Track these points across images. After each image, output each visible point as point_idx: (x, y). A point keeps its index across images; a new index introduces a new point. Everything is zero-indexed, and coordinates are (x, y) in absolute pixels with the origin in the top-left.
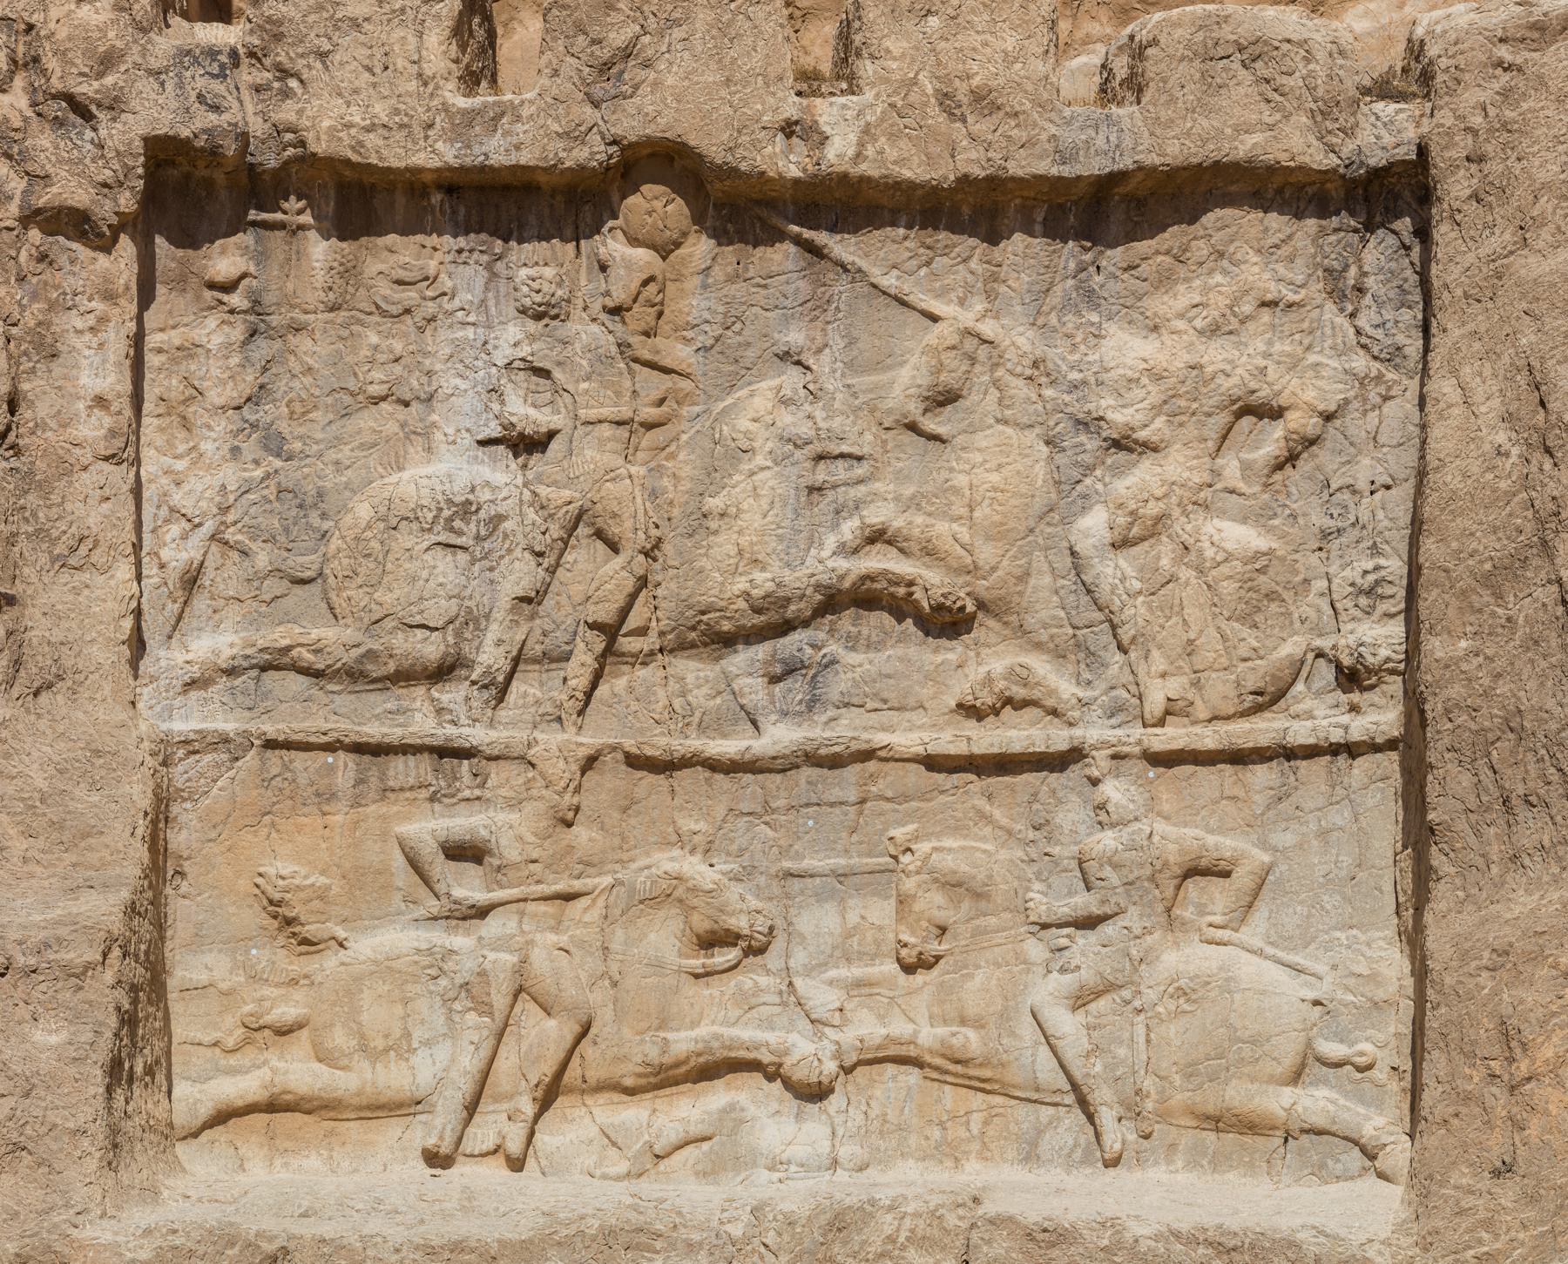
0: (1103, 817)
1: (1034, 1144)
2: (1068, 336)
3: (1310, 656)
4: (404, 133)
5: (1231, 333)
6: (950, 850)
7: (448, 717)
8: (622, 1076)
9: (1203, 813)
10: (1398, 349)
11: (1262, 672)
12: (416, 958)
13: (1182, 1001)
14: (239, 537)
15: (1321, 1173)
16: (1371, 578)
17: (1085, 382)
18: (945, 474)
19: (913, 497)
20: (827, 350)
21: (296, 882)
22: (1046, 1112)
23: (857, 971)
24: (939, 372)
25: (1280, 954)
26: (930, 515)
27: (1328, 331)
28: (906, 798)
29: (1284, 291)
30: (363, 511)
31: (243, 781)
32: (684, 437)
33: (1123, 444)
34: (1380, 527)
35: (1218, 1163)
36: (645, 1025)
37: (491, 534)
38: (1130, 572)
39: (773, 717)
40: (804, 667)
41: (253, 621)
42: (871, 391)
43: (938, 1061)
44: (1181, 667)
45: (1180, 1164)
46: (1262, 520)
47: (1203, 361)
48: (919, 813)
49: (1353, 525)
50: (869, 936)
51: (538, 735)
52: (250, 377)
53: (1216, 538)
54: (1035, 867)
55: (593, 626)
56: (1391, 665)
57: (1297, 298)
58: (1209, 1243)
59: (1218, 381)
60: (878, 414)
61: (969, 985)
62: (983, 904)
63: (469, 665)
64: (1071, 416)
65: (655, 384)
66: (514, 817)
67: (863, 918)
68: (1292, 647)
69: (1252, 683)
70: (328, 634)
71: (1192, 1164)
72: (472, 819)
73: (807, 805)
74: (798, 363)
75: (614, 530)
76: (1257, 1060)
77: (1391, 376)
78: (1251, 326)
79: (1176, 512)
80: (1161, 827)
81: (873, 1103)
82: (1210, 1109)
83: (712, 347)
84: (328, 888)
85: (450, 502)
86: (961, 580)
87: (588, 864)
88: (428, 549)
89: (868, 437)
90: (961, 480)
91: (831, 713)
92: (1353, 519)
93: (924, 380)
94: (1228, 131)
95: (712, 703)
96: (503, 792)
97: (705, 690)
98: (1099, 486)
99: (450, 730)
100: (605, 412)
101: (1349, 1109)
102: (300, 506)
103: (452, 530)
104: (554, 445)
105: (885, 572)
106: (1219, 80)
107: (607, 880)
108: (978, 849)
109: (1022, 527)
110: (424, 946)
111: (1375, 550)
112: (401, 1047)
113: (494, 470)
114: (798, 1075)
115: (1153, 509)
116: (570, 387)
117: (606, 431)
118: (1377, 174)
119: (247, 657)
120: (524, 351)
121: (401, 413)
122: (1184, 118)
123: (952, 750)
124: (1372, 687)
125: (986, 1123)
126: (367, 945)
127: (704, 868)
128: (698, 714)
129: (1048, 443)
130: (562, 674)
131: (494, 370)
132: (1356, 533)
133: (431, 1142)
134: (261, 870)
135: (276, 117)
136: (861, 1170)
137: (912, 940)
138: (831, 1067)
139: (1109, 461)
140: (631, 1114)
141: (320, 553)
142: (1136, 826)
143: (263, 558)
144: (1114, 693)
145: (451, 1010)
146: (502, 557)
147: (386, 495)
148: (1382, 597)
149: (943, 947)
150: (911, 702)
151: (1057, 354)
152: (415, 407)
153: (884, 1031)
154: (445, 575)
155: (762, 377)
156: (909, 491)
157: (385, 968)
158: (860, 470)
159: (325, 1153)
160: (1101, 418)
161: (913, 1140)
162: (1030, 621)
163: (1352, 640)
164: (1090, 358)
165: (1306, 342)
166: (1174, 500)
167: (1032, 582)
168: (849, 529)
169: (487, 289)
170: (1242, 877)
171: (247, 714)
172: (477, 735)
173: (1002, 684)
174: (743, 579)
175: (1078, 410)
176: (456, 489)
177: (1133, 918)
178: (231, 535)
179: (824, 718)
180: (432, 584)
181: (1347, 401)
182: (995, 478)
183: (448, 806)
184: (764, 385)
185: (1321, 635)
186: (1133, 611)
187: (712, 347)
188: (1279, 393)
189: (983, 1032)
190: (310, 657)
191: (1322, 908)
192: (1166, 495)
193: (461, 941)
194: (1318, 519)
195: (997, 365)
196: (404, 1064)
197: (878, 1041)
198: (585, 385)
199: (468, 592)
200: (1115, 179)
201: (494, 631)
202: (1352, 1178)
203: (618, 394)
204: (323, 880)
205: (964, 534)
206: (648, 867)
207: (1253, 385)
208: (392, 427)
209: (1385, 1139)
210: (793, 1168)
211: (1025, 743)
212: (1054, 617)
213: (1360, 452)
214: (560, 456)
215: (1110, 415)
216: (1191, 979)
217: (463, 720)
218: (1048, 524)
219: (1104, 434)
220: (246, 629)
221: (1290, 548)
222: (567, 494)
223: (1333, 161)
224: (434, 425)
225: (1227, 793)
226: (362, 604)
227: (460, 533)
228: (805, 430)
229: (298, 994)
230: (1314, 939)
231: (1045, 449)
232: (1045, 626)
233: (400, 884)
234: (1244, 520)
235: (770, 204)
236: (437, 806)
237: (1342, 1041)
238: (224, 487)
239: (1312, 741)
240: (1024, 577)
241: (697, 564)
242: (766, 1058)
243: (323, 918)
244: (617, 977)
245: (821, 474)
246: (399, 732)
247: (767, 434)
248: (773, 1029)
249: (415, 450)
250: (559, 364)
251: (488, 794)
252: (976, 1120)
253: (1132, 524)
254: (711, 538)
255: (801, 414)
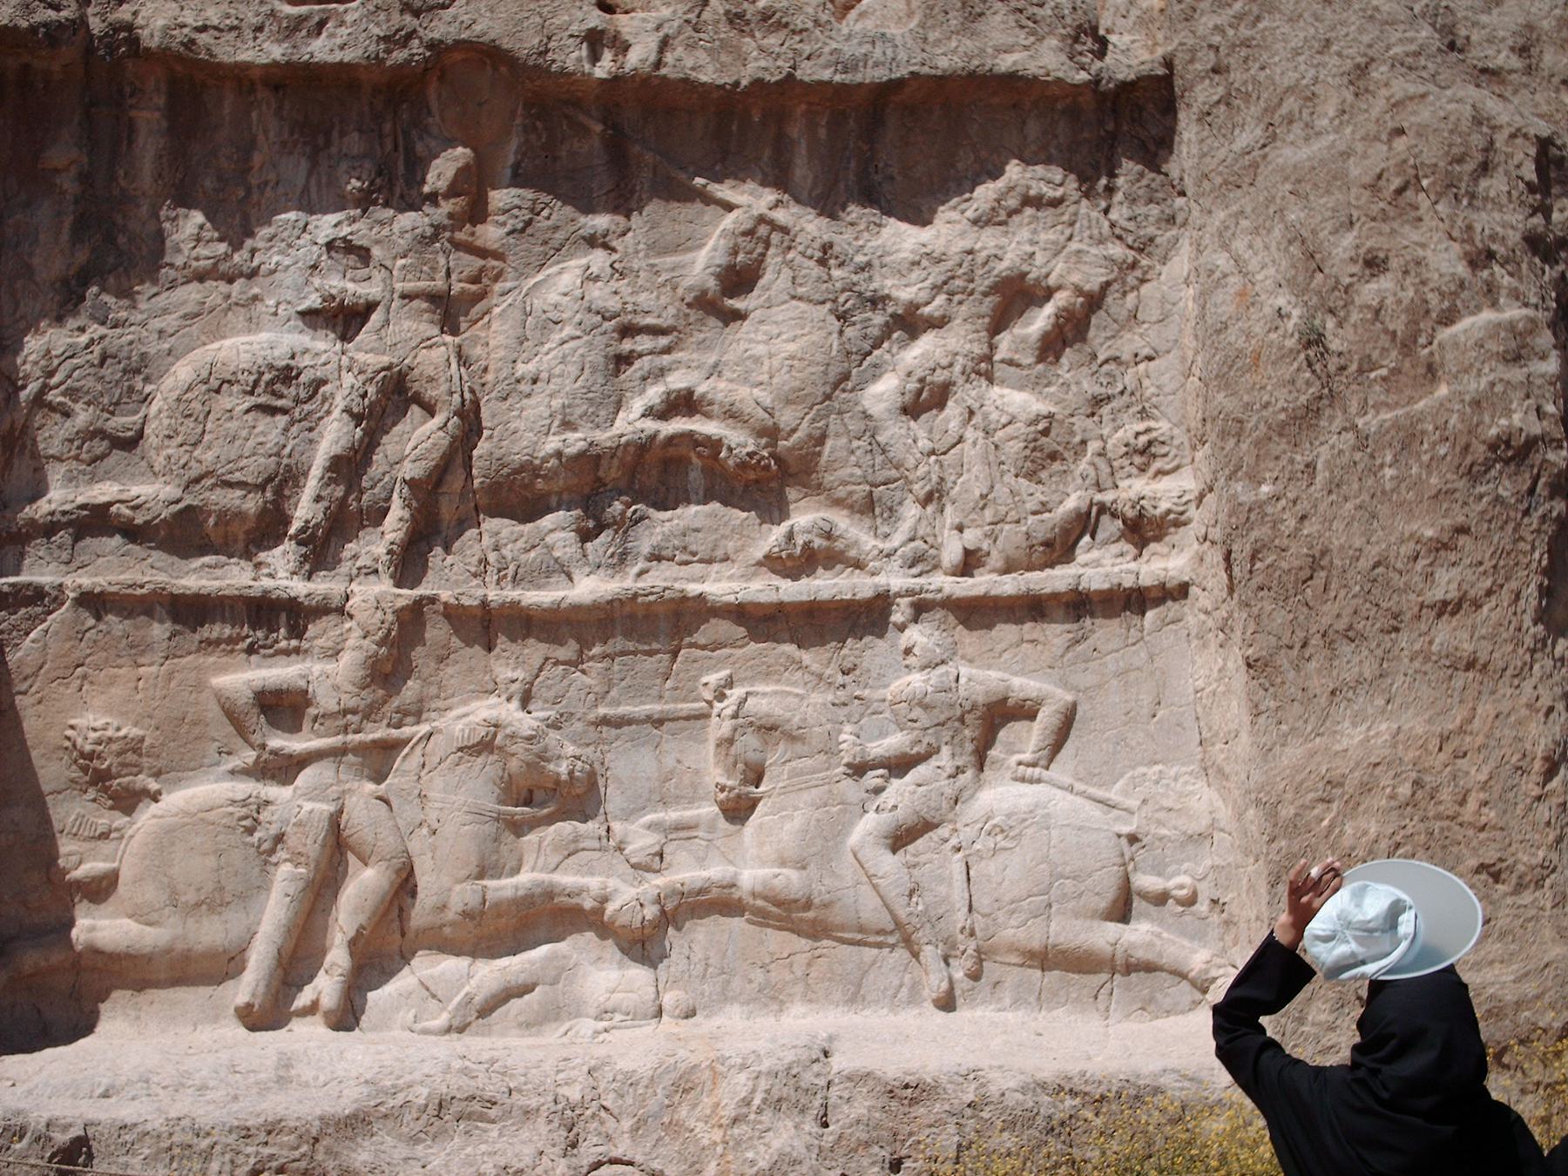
0: (911, 660)
1: (859, 986)
2: (852, 224)
3: (1094, 510)
4: (234, 34)
5: (1000, 224)
6: (764, 694)
7: (266, 571)
8: (441, 926)
9: (1006, 656)
10: (1152, 240)
11: (1050, 525)
12: (230, 809)
13: (999, 837)
14: (60, 399)
15: (1148, 1006)
16: (1143, 439)
17: (869, 264)
18: (743, 346)
19: (716, 365)
20: (630, 234)
21: (110, 733)
22: (869, 953)
23: (672, 815)
24: (735, 253)
25: (1092, 791)
26: (731, 381)
27: (1085, 223)
28: (716, 646)
29: (1045, 189)
30: (183, 372)
31: (57, 633)
32: (497, 310)
33: (910, 323)
34: (1148, 393)
35: (1042, 1000)
36: (465, 873)
37: (311, 398)
38: (922, 434)
39: (587, 569)
40: (615, 523)
41: (70, 479)
42: (673, 269)
43: (760, 903)
44: (973, 520)
45: (1008, 1001)
46: (1038, 389)
47: (977, 247)
48: (732, 660)
49: (1122, 393)
50: (686, 781)
51: (354, 586)
52: (82, 257)
53: (998, 403)
54: (846, 710)
55: (411, 483)
56: (1172, 516)
57: (1059, 193)
58: (1073, 1093)
59: (991, 264)
60: (680, 291)
61: (787, 826)
62: (799, 748)
63: (287, 521)
64: (860, 294)
65: (472, 263)
66: (330, 667)
67: (679, 761)
68: (1073, 502)
69: (1041, 534)
70: (142, 490)
71: (1017, 1003)
72: (290, 670)
73: (623, 653)
74: (606, 246)
75: (431, 393)
76: (1080, 895)
77: (1145, 262)
78: (1016, 219)
79: (961, 381)
80: (965, 671)
81: (696, 948)
82: (1036, 944)
83: (523, 230)
84: (142, 740)
85: (271, 367)
86: (764, 441)
87: (406, 714)
88: (248, 411)
89: (672, 310)
90: (760, 350)
91: (641, 565)
92: (1120, 387)
93: (722, 259)
94: (990, 51)
95: (523, 557)
96: (320, 642)
97: (520, 544)
98: (887, 357)
99: (267, 583)
100: (422, 284)
101: (1174, 943)
102: (125, 371)
103: (274, 393)
104: (376, 317)
105: (690, 435)
106: (978, 10)
107: (424, 729)
108: (789, 693)
109: (820, 391)
110: (240, 796)
111: (1144, 414)
112: (213, 903)
113: (313, 339)
114: (622, 920)
115: (940, 377)
116: (388, 263)
117: (423, 305)
118: (1125, 86)
119: (64, 513)
120: (345, 230)
121: (223, 287)
122: (949, 38)
123: (764, 598)
124: (1158, 539)
125: (809, 965)
126: (178, 799)
127: (521, 714)
128: (512, 568)
129: (838, 318)
130: (381, 529)
131: (315, 248)
132: (1126, 398)
133: (242, 998)
134: (72, 722)
135: (112, 17)
136: (687, 1017)
137: (730, 783)
138: (651, 912)
139: (895, 335)
140: (450, 966)
141: (141, 414)
142: (942, 669)
143: (83, 416)
144: (912, 544)
145: (266, 862)
146: (321, 418)
147: (209, 360)
148: (1155, 456)
149: (761, 789)
150: (719, 553)
151: (843, 239)
152: (239, 284)
153: (705, 874)
154: (263, 433)
155: (572, 256)
156: (712, 359)
157: (198, 819)
158: (663, 341)
159: (133, 1013)
160: (888, 297)
161: (736, 983)
162: (829, 478)
163: (1132, 494)
164: (873, 243)
165: (1068, 232)
166: (957, 368)
167: (829, 443)
168: (654, 394)
169: (310, 174)
170: (1047, 717)
171: (63, 568)
172: (299, 588)
173: (806, 537)
174: (556, 438)
175: (868, 288)
176: (276, 353)
177: (945, 759)
178: (54, 397)
179: (636, 570)
180: (251, 443)
181: (1108, 284)
182: (792, 347)
183: (264, 656)
184: (573, 263)
185: (1100, 491)
186: (926, 468)
187: (523, 230)
188: (1047, 276)
189: (804, 873)
190: (128, 512)
191: (1127, 745)
192: (951, 365)
193: (272, 791)
194: (1090, 387)
195: (789, 248)
196: (216, 917)
197: (698, 885)
198: (403, 261)
199: (287, 451)
200: (895, 85)
201: (311, 485)
202: (1182, 1012)
203: (433, 269)
204: (135, 732)
205: (765, 397)
206: (465, 715)
207: (1025, 268)
208: (215, 299)
209: (1214, 973)
210: (618, 1017)
211: (834, 591)
212: (852, 475)
213: (1122, 328)
214: (378, 325)
215: (895, 293)
216: (1009, 816)
217: (281, 574)
218: (844, 391)
219: (890, 310)
220: (66, 487)
221: (1067, 412)
222: (385, 360)
223: (1083, 76)
224: (255, 298)
225: (1027, 637)
226: (182, 462)
227: (281, 396)
228: (613, 304)
229: (105, 847)
230: (1122, 775)
231: (837, 324)
232: (844, 483)
233: (215, 735)
234: (1021, 388)
235: (577, 103)
236: (254, 658)
237: (1159, 874)
238: (48, 351)
239: (1106, 586)
240: (821, 440)
241: (512, 426)
242: (588, 904)
243: (135, 770)
244: (435, 825)
245: (627, 346)
246: (217, 584)
247: (576, 307)
248: (592, 874)
249: (237, 318)
250: (377, 242)
251: (305, 645)
252: (800, 959)
253: (919, 392)
254: (525, 401)
255: (608, 290)
